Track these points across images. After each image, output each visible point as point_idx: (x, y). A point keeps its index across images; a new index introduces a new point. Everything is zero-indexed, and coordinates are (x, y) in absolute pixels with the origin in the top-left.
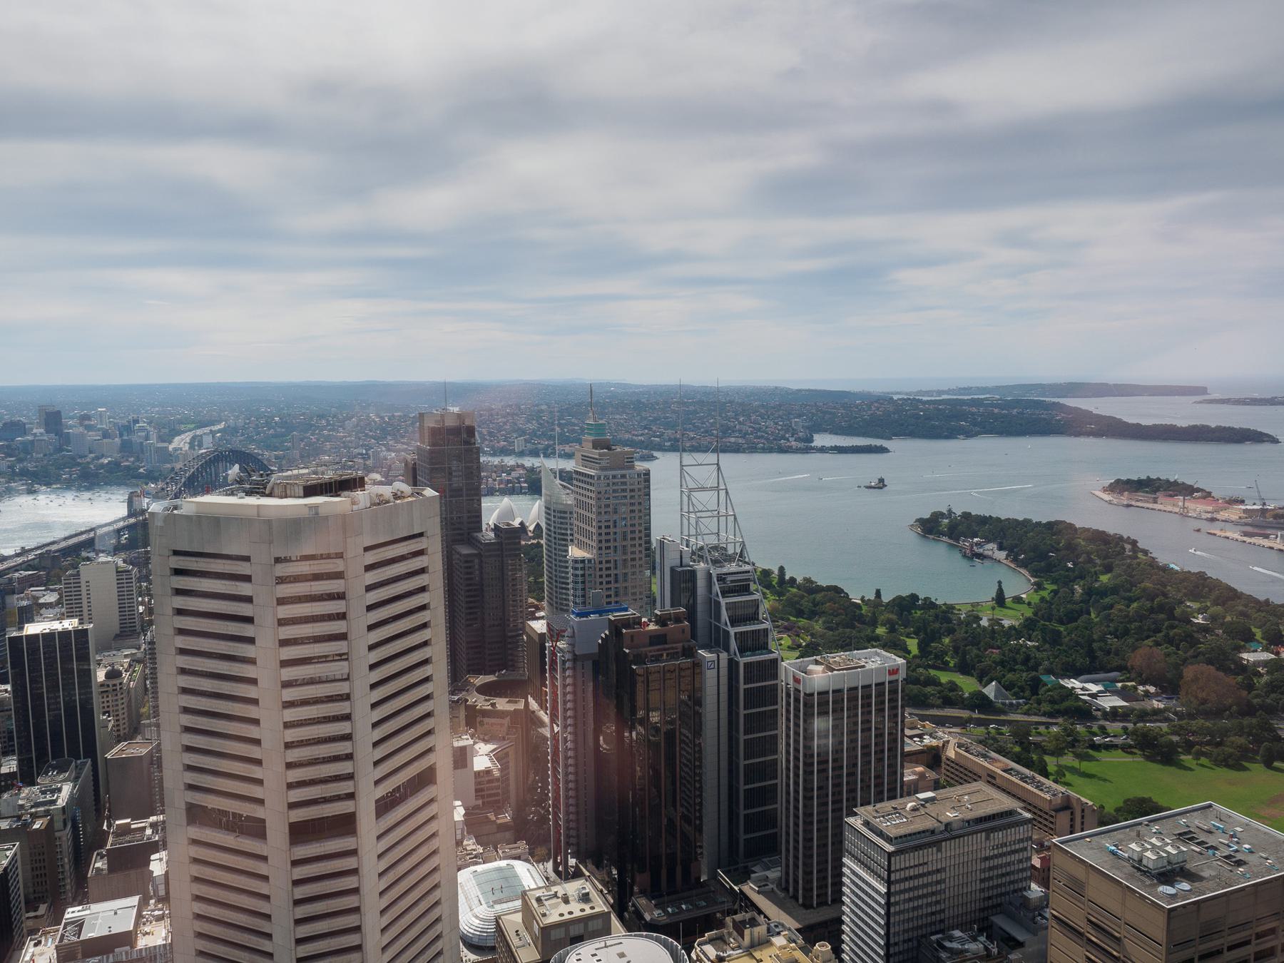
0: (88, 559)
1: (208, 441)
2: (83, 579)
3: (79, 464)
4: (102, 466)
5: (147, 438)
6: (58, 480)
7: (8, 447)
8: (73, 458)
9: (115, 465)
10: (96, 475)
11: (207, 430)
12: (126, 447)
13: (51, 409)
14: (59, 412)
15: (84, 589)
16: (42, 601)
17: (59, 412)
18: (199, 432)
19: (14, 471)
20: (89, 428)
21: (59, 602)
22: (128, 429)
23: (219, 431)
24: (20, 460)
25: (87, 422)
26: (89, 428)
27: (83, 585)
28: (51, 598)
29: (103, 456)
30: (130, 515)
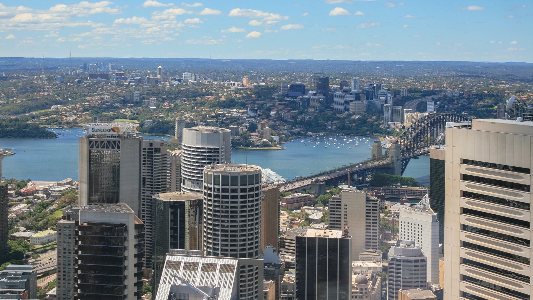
1: (431, 106)
3: (339, 119)
4: (354, 121)
5: (386, 102)
6: (324, 130)
7: (293, 102)
9: (363, 121)
10: (349, 128)
11: (430, 98)
14: (327, 79)
16: (310, 217)
17: (327, 79)
18: (424, 99)
19: (296, 120)
20: (347, 92)
22: (370, 95)
23: (439, 99)
24: (301, 113)
26: (347, 92)
27: (343, 207)
28: (318, 215)
29: (354, 114)
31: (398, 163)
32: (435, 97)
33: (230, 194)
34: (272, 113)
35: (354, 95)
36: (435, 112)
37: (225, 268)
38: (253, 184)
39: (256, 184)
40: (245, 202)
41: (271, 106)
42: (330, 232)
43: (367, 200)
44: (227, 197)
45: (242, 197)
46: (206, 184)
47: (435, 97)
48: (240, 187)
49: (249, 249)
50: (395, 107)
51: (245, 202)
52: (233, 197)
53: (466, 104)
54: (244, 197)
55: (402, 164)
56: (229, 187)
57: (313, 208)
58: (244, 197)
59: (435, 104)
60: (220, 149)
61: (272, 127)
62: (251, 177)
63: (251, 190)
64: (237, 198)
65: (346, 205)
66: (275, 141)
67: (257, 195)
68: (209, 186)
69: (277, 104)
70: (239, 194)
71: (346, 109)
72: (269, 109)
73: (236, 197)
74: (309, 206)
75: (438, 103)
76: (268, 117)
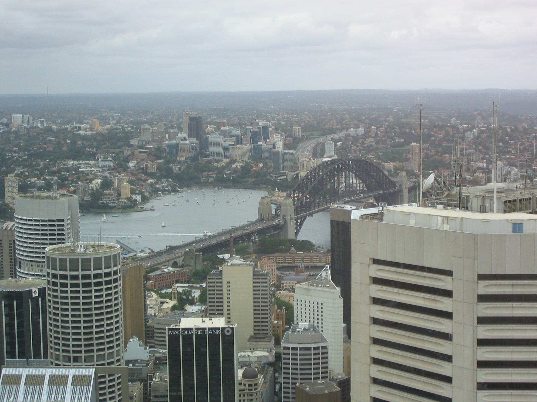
0: (223, 261)
1: (330, 149)
2: (225, 279)
4: (235, 171)
7: (158, 149)
8: (210, 162)
9: (246, 170)
11: (329, 137)
12: (256, 154)
13: (195, 114)
15: (225, 288)
18: (321, 139)
21: (203, 300)
23: (339, 140)
25: (223, 128)
27: (225, 285)
29: (235, 161)
30: (261, 219)
31: (292, 224)
32: (336, 136)
33: (81, 281)
34: (132, 165)
35: (234, 138)
36: (336, 157)
37: (78, 380)
38: (110, 267)
39: (114, 267)
40: (101, 290)
41: (129, 155)
42: (210, 319)
43: (254, 275)
44: (77, 285)
45: (97, 284)
46: (49, 271)
47: (336, 136)
48: (93, 272)
49: (109, 348)
50: (285, 151)
51: (101, 290)
52: (84, 285)
53: (373, 144)
54: (100, 284)
55: (297, 225)
56: (80, 273)
57: (187, 285)
58: (100, 284)
59: (335, 145)
60: (66, 221)
61: (131, 182)
62: (107, 258)
63: (108, 275)
64: (91, 286)
65: (228, 282)
66: (136, 200)
67: (116, 280)
68: (54, 272)
69: (137, 152)
70: (93, 281)
71: (225, 157)
72: (127, 160)
73: (89, 285)
74: (182, 283)
75: (339, 144)
76: (126, 169)
